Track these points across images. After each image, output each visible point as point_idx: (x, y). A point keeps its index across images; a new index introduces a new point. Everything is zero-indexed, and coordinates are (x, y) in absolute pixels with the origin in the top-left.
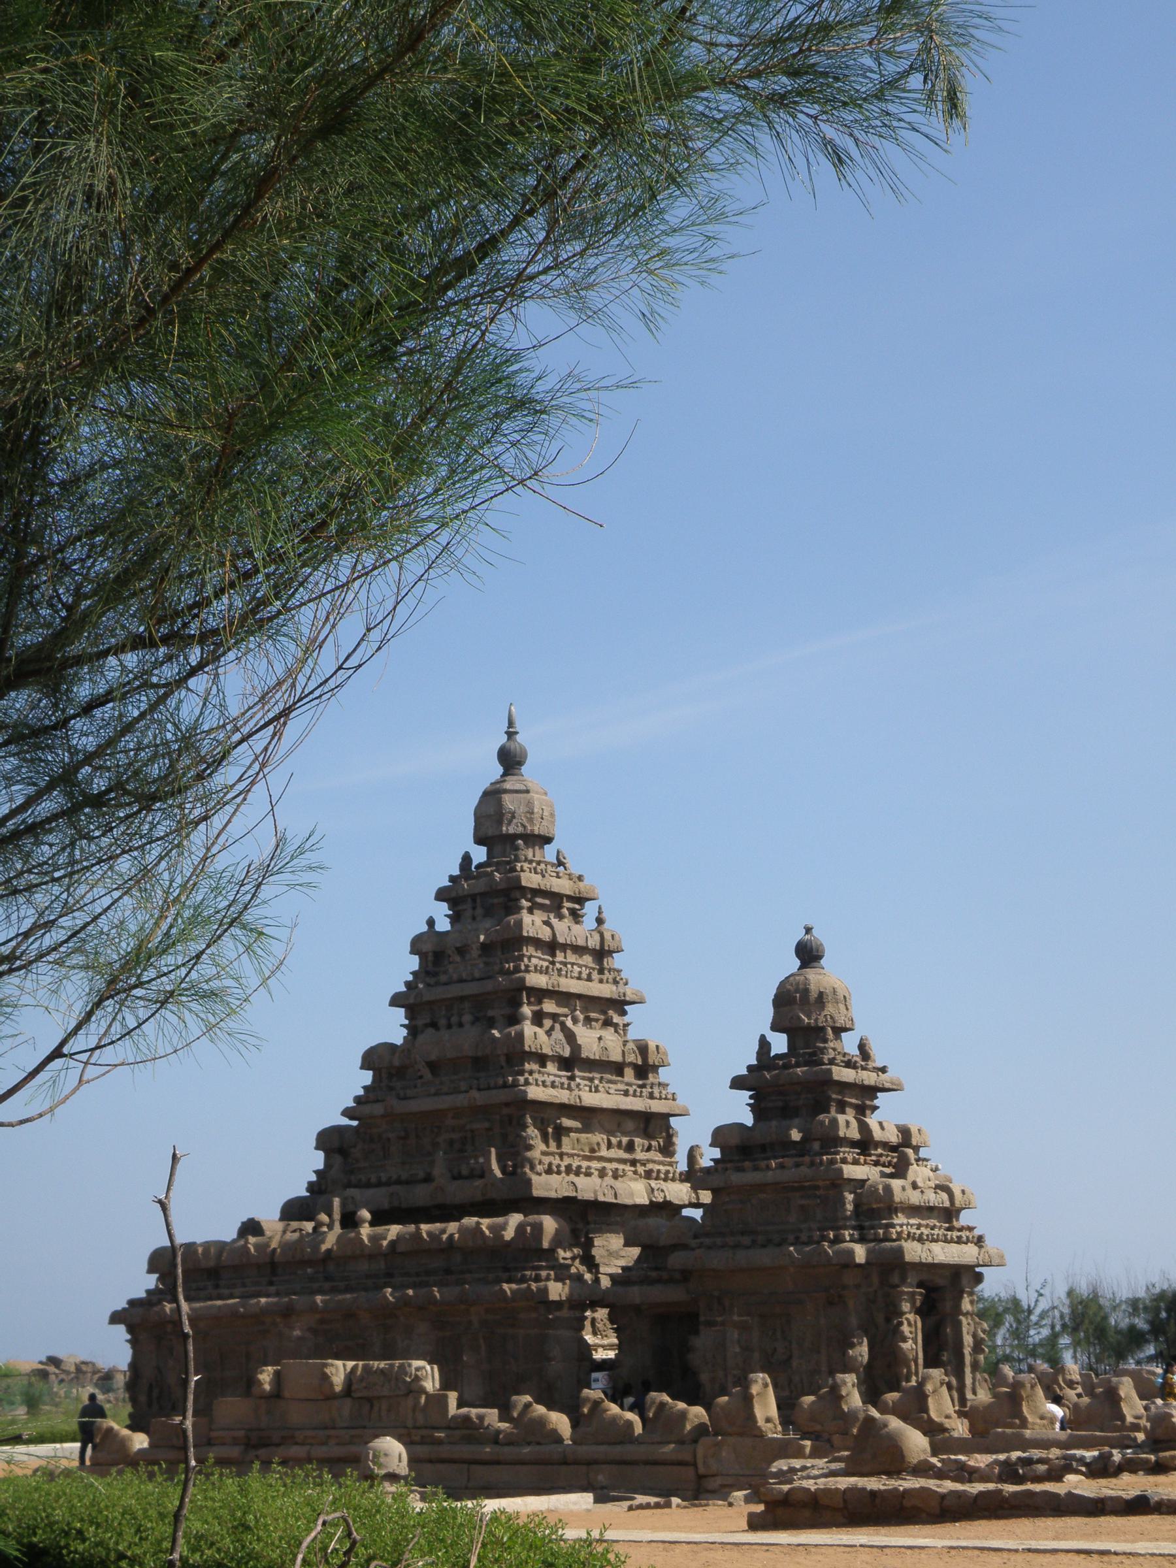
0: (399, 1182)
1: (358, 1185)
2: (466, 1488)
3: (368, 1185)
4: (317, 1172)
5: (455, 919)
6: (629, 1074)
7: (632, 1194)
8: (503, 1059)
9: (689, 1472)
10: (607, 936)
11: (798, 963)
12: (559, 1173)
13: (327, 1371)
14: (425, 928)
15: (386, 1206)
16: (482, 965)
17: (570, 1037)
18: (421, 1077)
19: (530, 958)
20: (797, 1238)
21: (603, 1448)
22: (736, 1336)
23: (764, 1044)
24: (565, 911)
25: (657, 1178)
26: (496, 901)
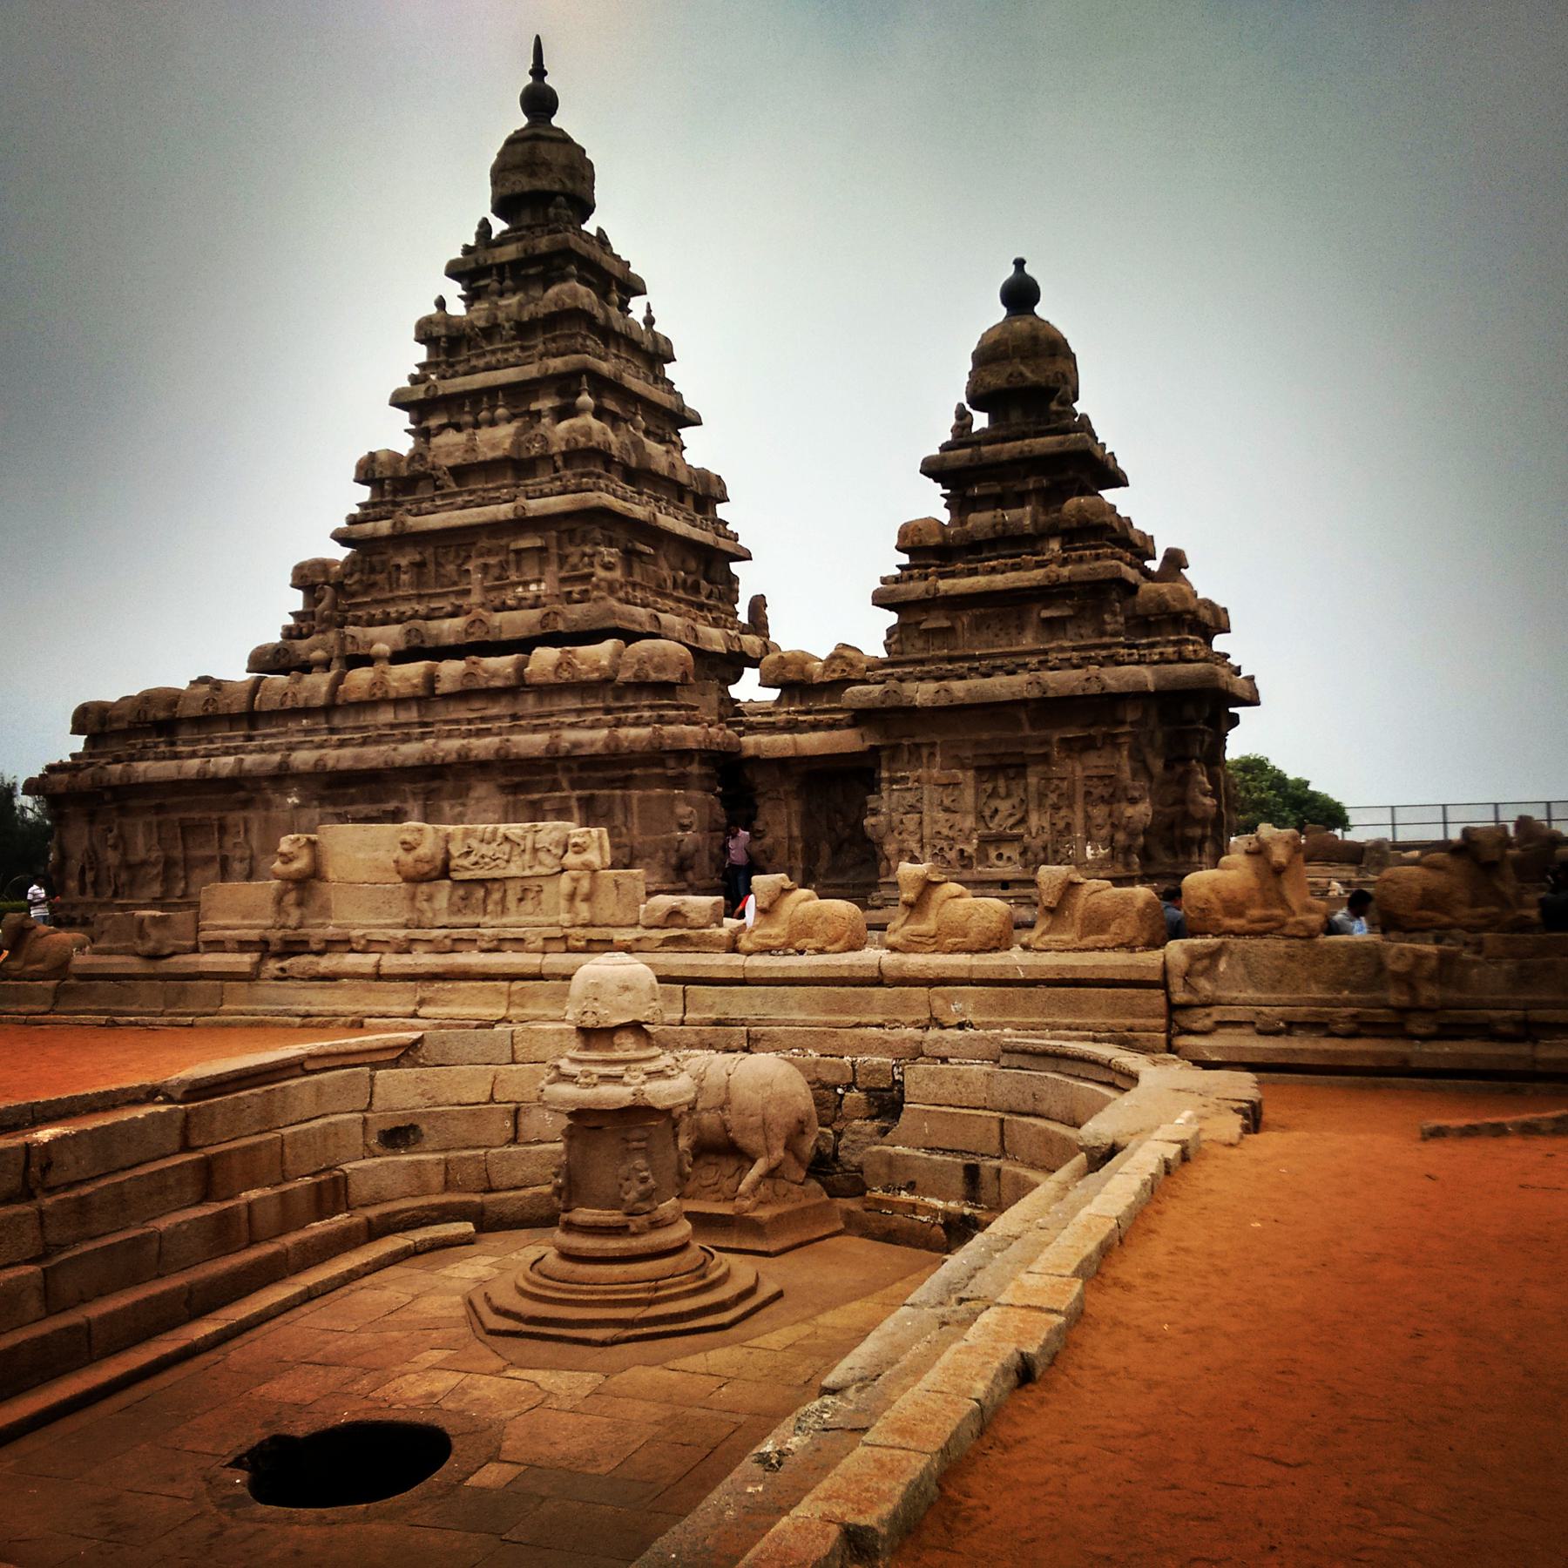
0: (412, 617)
1: (355, 624)
2: (682, 1023)
3: (371, 622)
4: (295, 615)
5: (470, 299)
6: (689, 504)
7: (710, 640)
8: (560, 463)
9: (1157, 997)
10: (662, 341)
11: (1003, 311)
12: (635, 604)
13: (408, 838)
14: (433, 310)
15: (402, 646)
16: (517, 351)
17: (638, 445)
18: (437, 488)
19: (585, 338)
20: (1040, 662)
21: (962, 959)
22: (936, 795)
23: (961, 414)
24: (615, 297)
25: (725, 627)
26: (532, 271)
